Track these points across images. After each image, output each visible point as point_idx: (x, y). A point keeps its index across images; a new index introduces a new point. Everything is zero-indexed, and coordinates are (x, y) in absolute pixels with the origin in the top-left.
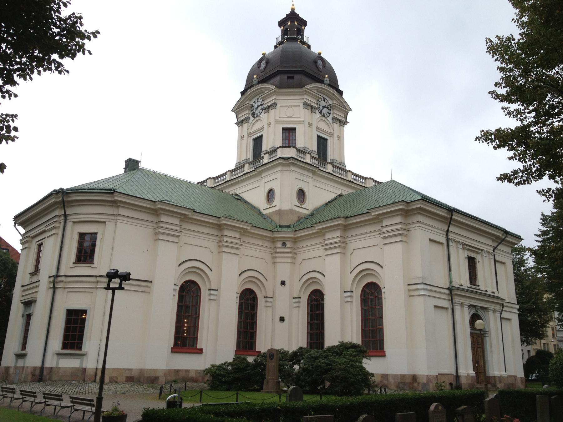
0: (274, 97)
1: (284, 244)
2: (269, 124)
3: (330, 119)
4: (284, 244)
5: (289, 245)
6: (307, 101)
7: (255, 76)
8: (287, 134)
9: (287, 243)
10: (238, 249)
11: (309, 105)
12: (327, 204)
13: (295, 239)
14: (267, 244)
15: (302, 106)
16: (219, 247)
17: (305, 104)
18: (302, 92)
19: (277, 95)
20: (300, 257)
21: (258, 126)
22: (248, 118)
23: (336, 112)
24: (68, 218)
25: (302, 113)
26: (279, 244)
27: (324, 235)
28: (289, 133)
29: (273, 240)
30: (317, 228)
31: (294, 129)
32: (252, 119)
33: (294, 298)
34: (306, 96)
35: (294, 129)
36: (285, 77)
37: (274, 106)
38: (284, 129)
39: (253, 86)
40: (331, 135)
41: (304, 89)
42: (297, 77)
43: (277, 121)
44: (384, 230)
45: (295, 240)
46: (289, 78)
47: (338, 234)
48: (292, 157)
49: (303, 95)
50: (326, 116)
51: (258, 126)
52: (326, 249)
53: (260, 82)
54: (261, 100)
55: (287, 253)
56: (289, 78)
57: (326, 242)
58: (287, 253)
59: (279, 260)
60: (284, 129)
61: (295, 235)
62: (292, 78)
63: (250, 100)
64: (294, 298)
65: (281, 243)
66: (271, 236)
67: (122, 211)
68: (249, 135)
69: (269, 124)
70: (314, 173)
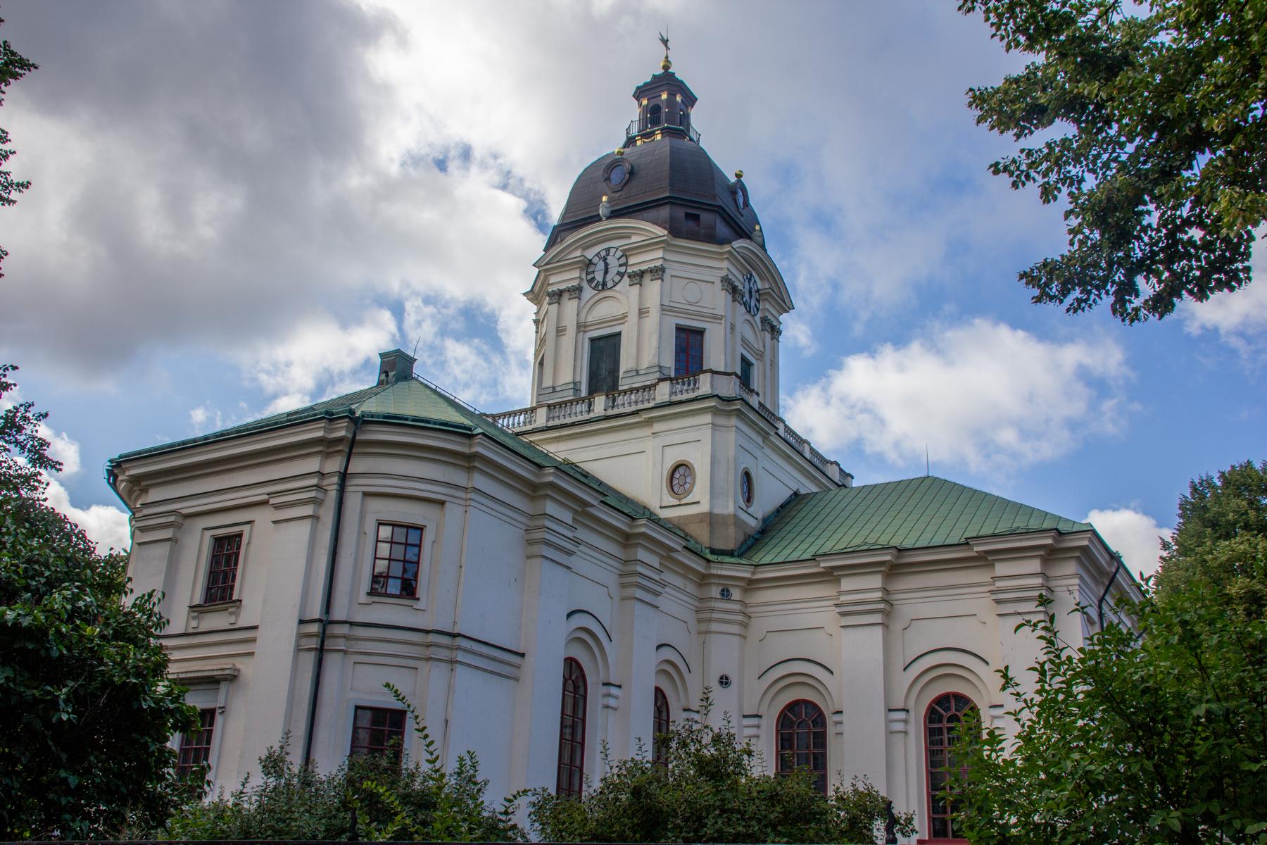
0: (660, 254)
1: (725, 594)
2: (642, 312)
3: (758, 318)
4: (725, 594)
5: (736, 594)
7: (604, 199)
9: (732, 590)
12: (778, 511)
13: (751, 582)
14: (690, 588)
15: (718, 285)
16: (623, 586)
17: (726, 280)
18: (722, 254)
20: (761, 624)
21: (605, 310)
22: (579, 289)
23: (768, 306)
24: (351, 482)
25: (718, 300)
26: (715, 592)
27: (837, 580)
29: (703, 580)
31: (700, 333)
32: (588, 292)
33: (744, 716)
34: (725, 264)
35: (700, 333)
36: (680, 213)
37: (658, 272)
38: (679, 329)
39: (597, 218)
40: (760, 355)
41: (727, 248)
42: (706, 217)
44: (999, 584)
45: (751, 585)
46: (688, 216)
47: (876, 581)
48: (717, 396)
51: (605, 310)
52: (843, 614)
53: (615, 214)
54: (619, 254)
55: (733, 612)
57: (843, 598)
58: (733, 612)
59: (714, 627)
60: (679, 329)
61: (754, 573)
62: (696, 218)
63: (585, 248)
64: (744, 716)
65: (720, 589)
66: (703, 571)
67: (479, 481)
68: (581, 327)
70: (765, 436)
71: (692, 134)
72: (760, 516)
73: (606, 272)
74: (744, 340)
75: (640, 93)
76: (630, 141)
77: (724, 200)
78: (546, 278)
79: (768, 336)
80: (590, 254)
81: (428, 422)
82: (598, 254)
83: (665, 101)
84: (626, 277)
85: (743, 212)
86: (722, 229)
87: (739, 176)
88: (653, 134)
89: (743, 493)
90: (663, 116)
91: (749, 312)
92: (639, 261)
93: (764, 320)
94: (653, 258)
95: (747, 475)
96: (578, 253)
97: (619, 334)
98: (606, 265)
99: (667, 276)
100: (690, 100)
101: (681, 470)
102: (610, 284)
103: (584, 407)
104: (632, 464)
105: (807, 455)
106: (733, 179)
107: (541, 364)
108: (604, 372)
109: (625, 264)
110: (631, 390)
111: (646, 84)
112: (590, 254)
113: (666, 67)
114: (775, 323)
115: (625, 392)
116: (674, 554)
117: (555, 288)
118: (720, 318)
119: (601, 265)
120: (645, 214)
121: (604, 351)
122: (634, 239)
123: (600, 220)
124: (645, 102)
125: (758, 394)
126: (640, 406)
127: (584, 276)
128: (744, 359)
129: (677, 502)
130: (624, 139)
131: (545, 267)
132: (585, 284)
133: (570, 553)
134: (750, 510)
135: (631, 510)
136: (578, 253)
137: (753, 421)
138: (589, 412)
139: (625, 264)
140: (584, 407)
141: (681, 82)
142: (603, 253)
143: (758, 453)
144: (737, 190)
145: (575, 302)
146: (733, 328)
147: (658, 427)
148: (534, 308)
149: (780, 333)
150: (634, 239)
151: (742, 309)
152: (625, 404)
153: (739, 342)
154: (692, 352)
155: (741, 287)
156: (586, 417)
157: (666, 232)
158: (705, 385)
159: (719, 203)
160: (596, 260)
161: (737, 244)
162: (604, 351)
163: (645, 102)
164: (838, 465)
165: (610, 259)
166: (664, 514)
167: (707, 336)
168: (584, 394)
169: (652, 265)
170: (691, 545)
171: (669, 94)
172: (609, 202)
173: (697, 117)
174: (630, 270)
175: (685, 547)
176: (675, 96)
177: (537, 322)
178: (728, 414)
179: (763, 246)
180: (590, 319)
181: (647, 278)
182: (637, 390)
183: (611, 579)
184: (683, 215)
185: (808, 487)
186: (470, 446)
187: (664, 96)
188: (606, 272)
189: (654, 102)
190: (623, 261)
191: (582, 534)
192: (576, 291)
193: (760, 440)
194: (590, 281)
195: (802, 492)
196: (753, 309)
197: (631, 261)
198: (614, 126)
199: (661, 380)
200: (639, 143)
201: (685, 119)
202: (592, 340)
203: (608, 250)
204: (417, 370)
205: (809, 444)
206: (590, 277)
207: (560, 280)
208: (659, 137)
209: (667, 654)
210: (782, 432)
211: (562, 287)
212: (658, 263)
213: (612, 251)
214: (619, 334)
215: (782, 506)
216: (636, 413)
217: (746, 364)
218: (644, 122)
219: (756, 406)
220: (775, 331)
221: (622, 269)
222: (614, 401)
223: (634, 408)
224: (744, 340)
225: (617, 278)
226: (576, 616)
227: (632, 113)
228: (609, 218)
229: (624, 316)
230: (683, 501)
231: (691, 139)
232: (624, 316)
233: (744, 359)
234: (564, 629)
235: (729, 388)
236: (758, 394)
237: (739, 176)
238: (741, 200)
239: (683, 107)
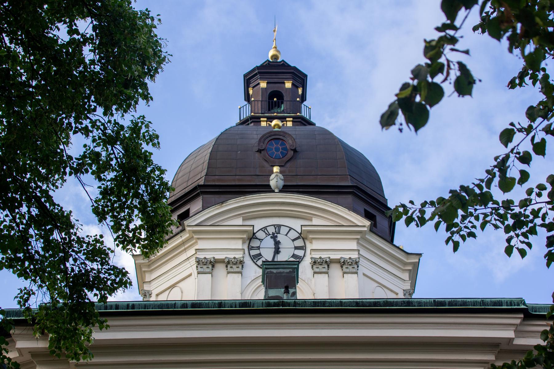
37: (349, 265)
53: (286, 189)
73: (277, 251)
80: (259, 224)
82: (264, 229)
94: (347, 248)
96: (239, 221)
98: (277, 244)
109: (303, 248)
119: (269, 243)
120: (341, 198)
122: (316, 221)
132: (248, 261)
139: (303, 248)
142: (271, 230)
145: (237, 277)
150: (316, 221)
160: (261, 235)
165: (280, 238)
188: (277, 251)
189: (276, 87)
190: (299, 243)
203: (279, 226)
206: (253, 252)
208: (290, 124)
211: (220, 256)
212: (354, 256)
213: (284, 230)
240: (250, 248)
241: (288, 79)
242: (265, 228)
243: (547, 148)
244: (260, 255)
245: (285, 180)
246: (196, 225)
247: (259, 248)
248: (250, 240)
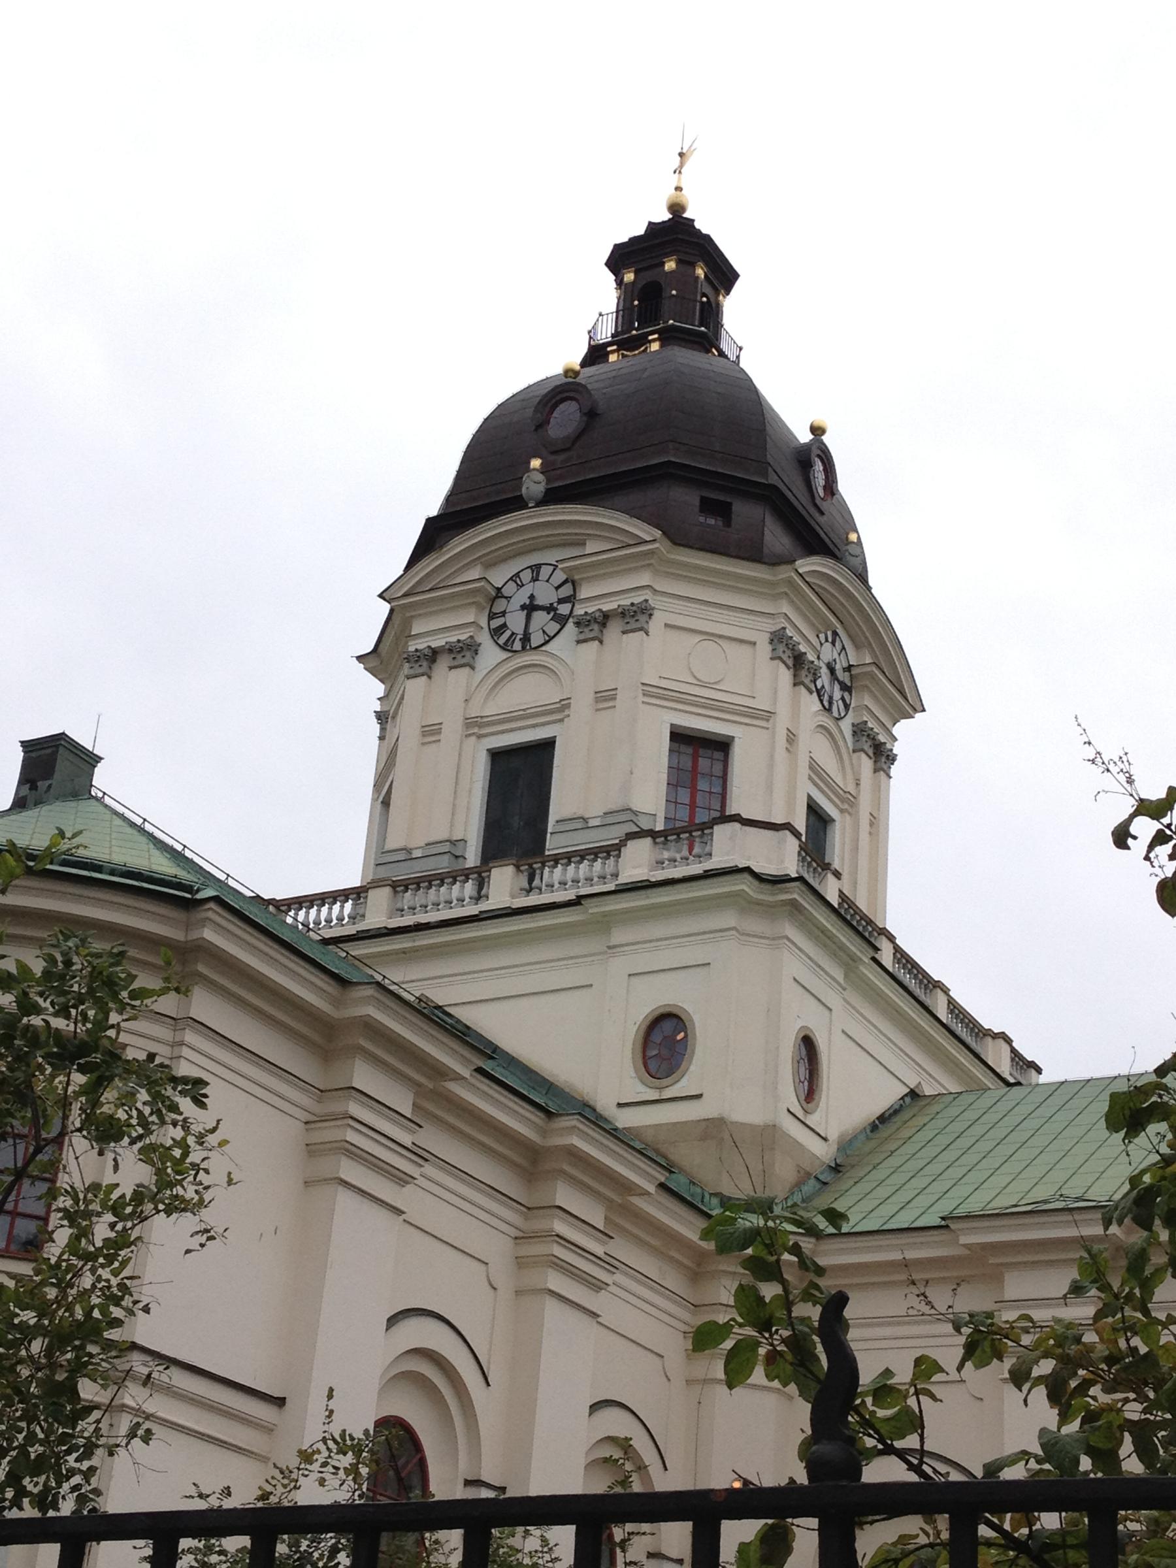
0: (644, 579)
2: (605, 698)
3: (846, 725)
6: (789, 633)
7: (536, 463)
8: (687, 762)
10: (597, 1286)
11: (792, 647)
14: (673, 1280)
15: (764, 648)
16: (521, 1263)
17: (778, 638)
18: (772, 584)
19: (656, 572)
21: (528, 691)
23: (868, 701)
28: (700, 754)
30: (964, 1240)
31: (723, 746)
32: (490, 654)
34: (786, 608)
35: (723, 746)
37: (635, 617)
38: (680, 737)
39: (517, 503)
40: (849, 802)
41: (785, 572)
42: (744, 511)
43: (655, 694)
48: (748, 870)
49: (776, 597)
50: (835, 714)
51: (528, 691)
53: (552, 497)
54: (559, 577)
56: (708, 507)
60: (680, 737)
62: (722, 510)
63: (488, 566)
68: (474, 725)
69: (605, 698)
70: (849, 964)
71: (724, 346)
72: (833, 1135)
74: (814, 766)
75: (619, 259)
76: (596, 354)
77: (787, 479)
78: (407, 623)
79: (866, 764)
80: (499, 577)
81: (98, 868)
82: (515, 578)
83: (671, 276)
84: (570, 625)
85: (824, 506)
86: (776, 537)
87: (817, 431)
88: (643, 340)
89: (797, 1082)
90: (666, 306)
91: (829, 710)
92: (597, 594)
93: (860, 730)
95: (808, 1043)
96: (474, 573)
97: (548, 745)
99: (656, 624)
100: (724, 276)
101: (667, 1026)
102: (536, 639)
103: (469, 888)
104: (562, 1015)
105: (942, 1013)
106: (804, 437)
107: (386, 803)
108: (516, 822)
109: (571, 599)
110: (568, 858)
111: (634, 241)
112: (499, 577)
113: (676, 209)
114: (882, 738)
115: (556, 859)
116: (637, 1201)
117: (421, 644)
118: (768, 715)
121: (520, 777)
122: (591, 547)
123: (525, 507)
124: (629, 277)
125: (837, 875)
126: (584, 891)
127: (483, 622)
128: (813, 809)
129: (653, 1095)
130: (582, 350)
131: (403, 601)
132: (484, 638)
133: (402, 1179)
134: (811, 1120)
135: (545, 1097)
136: (474, 573)
137: (824, 931)
138: (479, 898)
140: (469, 888)
141: (708, 238)
143: (833, 999)
144: (814, 458)
146: (791, 738)
147: (619, 936)
148: (379, 689)
149: (892, 759)
151: (812, 704)
152: (559, 882)
153: (804, 770)
154: (703, 785)
155: (811, 656)
156: (473, 910)
157: (658, 533)
158: (728, 846)
159: (773, 479)
161: (808, 565)
162: (520, 777)
163: (629, 277)
164: (1009, 1041)
166: (625, 1119)
167: (738, 752)
168: (472, 858)
169: (626, 601)
170: (678, 1183)
171: (679, 262)
172: (543, 470)
173: (738, 313)
174: (579, 610)
175: (662, 1186)
176: (693, 265)
177: (382, 717)
178: (768, 910)
179: (862, 577)
180: (492, 709)
181: (613, 631)
182: (582, 855)
183: (495, 1246)
184: (697, 502)
185: (935, 1081)
186: (188, 927)
187: (670, 265)
189: (649, 276)
190: (566, 591)
191: (432, 1139)
192: (463, 653)
193: (839, 975)
194: (496, 632)
195: (928, 1091)
196: (838, 706)
197: (584, 593)
198: (559, 320)
199: (631, 836)
200: (613, 358)
201: (712, 315)
202: (497, 756)
203: (536, 569)
204: (102, 779)
205: (946, 991)
206: (496, 623)
207: (431, 631)
208: (655, 346)
209: (616, 1424)
210: (887, 957)
211: (437, 642)
213: (545, 572)
214: (548, 745)
215: (883, 1119)
216: (578, 901)
217: (818, 818)
218: (625, 312)
219: (834, 901)
220: (882, 756)
221: (564, 609)
222: (531, 879)
223: (570, 895)
224: (814, 766)
225: (553, 627)
226: (413, 1323)
227: (597, 301)
228: (541, 503)
229: (564, 706)
230: (668, 1094)
231: (722, 354)
232: (564, 706)
233: (813, 809)
234: (377, 1351)
235: (783, 857)
236: (837, 875)
237: (817, 431)
238: (819, 480)
239: (707, 289)
240: (492, 616)
241: (668, 255)
242: (517, 575)
243: (454, 474)
244: (504, 626)
245: (548, 481)
246: (405, 595)
247: (504, 613)
248: (493, 600)
